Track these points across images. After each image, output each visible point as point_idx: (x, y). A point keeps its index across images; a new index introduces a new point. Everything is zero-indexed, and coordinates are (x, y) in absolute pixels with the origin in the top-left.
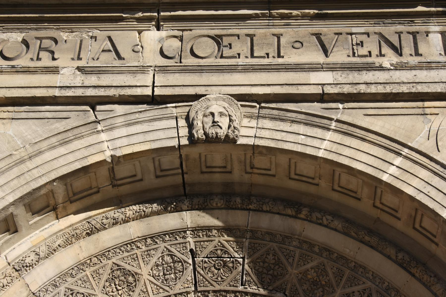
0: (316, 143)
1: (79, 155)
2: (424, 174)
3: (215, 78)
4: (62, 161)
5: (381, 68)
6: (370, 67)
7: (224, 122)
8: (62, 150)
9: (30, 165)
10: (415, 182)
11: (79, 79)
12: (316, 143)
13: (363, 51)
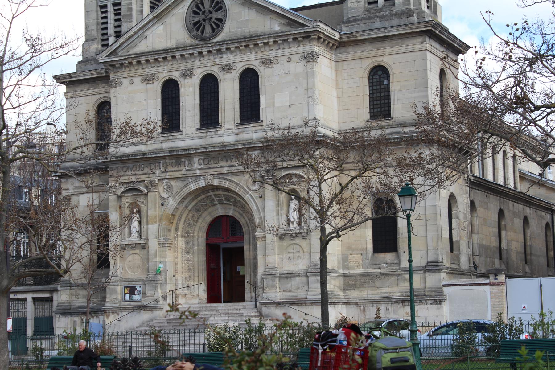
0: (225, 184)
1: (188, 189)
2: (242, 190)
3: (208, 171)
4: (186, 191)
5: (235, 166)
6: (233, 166)
7: (210, 181)
8: (186, 189)
9: (181, 192)
10: (241, 192)
11: (186, 173)
12: (225, 184)
13: (233, 161)
